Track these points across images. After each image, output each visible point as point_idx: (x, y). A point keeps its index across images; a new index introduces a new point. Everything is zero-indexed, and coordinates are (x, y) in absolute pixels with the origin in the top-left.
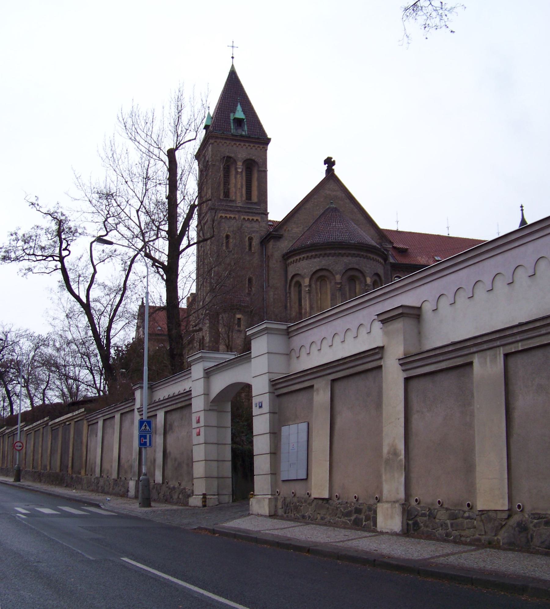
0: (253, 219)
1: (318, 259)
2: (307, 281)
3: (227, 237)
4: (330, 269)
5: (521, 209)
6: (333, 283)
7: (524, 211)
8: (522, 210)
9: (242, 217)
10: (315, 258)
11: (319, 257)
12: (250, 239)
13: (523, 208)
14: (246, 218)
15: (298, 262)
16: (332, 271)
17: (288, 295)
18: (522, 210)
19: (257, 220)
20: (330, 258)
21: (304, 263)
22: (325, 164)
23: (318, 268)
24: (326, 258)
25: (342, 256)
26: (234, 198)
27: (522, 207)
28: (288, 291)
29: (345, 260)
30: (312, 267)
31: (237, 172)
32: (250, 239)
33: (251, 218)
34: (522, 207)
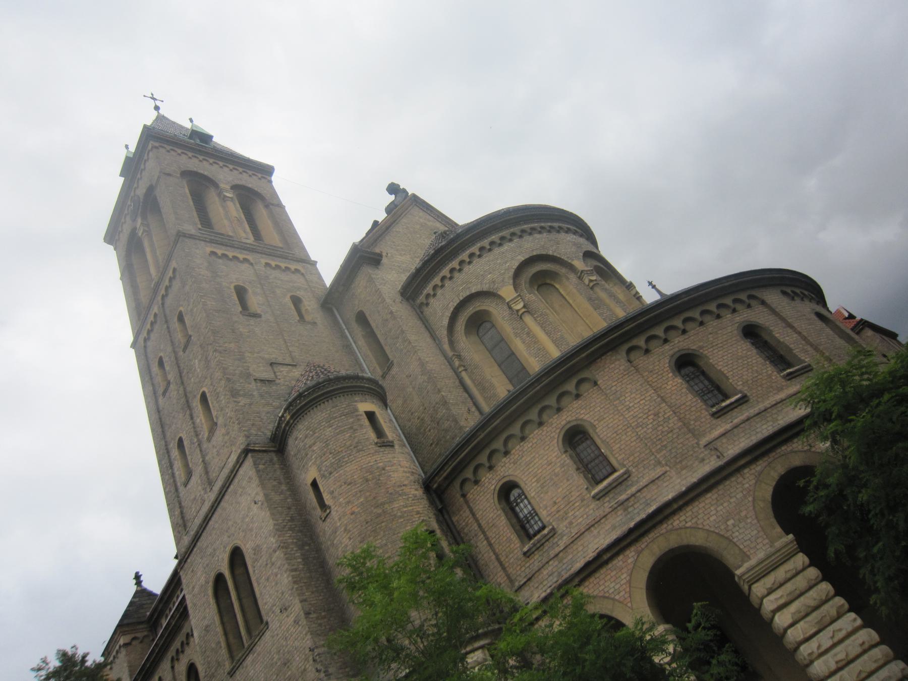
0: (287, 269)
1: (512, 245)
2: (508, 292)
3: (241, 292)
4: (550, 253)
5: (650, 287)
6: (573, 278)
7: (657, 287)
8: (654, 287)
9: (263, 261)
10: (500, 245)
11: (511, 240)
12: (296, 302)
13: (654, 283)
14: (273, 264)
15: (456, 274)
16: (555, 254)
17: (457, 363)
18: (654, 287)
19: (297, 271)
20: (537, 236)
21: (479, 267)
22: (391, 193)
23: (521, 258)
24: (527, 238)
25: (558, 232)
26: (231, 234)
27: (650, 283)
28: (450, 353)
29: (568, 238)
30: (506, 263)
31: (224, 199)
32: (296, 302)
33: (283, 265)
34: (650, 283)
